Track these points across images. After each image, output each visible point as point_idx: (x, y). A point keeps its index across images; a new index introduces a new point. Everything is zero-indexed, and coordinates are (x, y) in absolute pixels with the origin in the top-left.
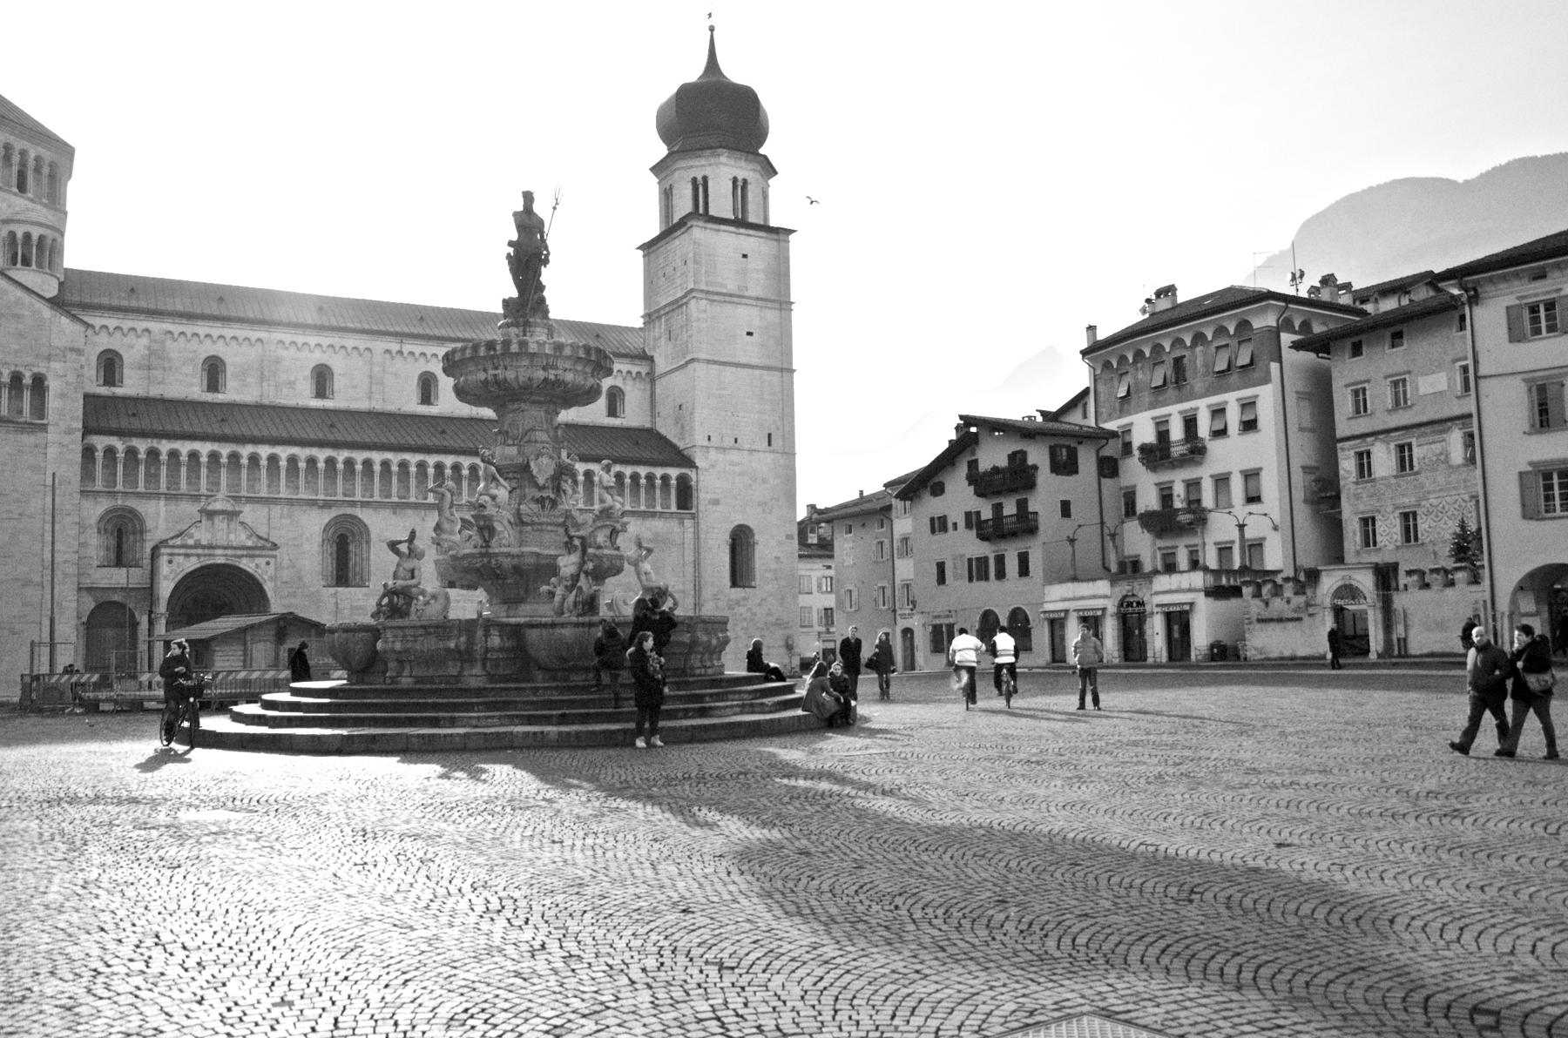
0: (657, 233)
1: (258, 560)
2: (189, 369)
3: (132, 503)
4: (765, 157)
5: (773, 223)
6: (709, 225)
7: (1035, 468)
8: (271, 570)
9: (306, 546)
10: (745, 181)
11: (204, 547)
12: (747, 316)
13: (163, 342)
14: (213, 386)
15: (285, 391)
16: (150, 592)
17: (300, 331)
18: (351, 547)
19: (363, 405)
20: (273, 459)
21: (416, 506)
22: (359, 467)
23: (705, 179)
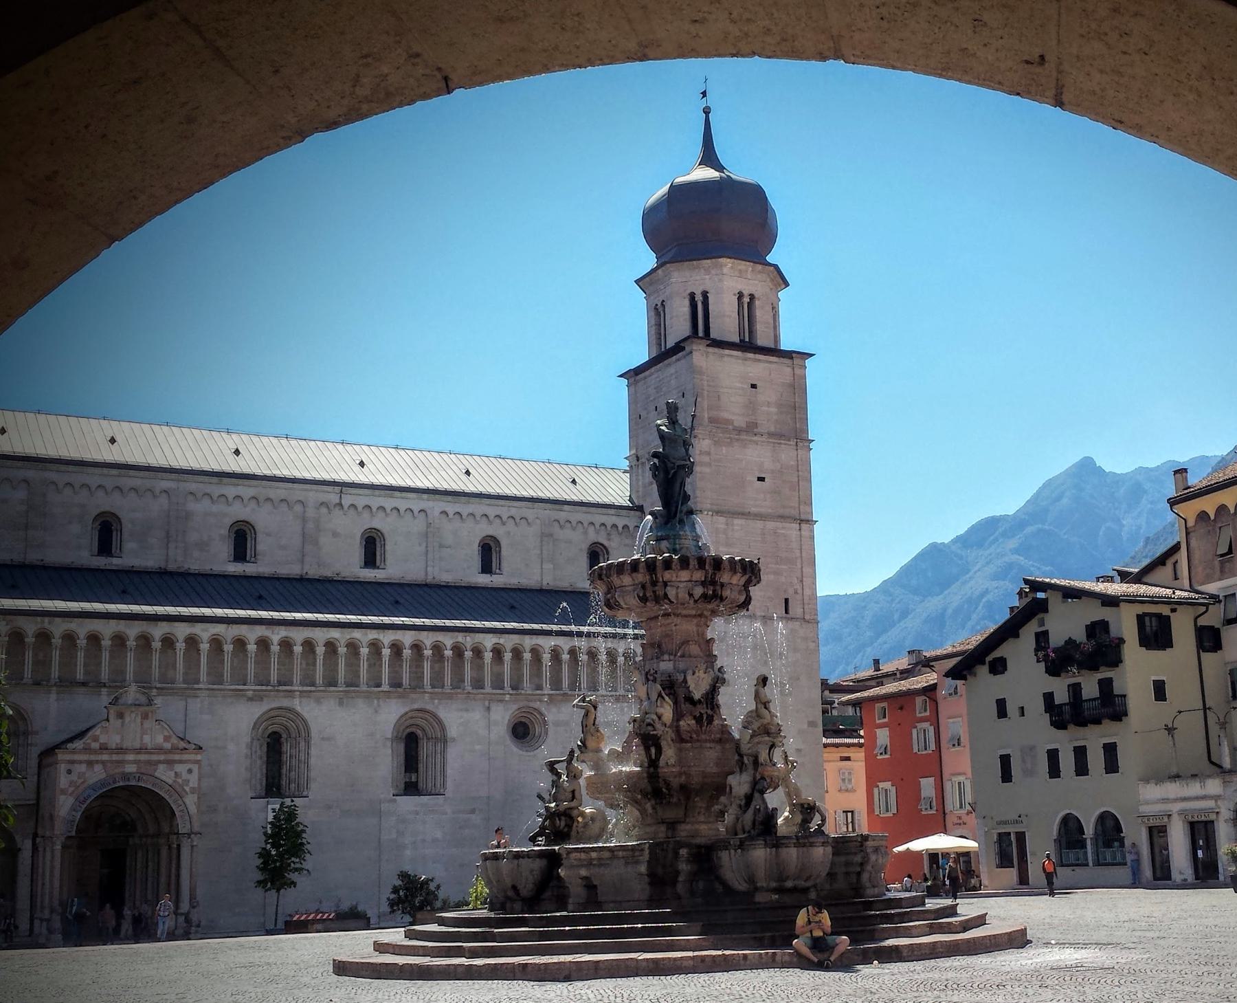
0: (645, 358)
1: (179, 768)
4: (776, 267)
5: (785, 345)
6: (711, 350)
7: (1122, 641)
8: (193, 781)
9: (231, 747)
10: (752, 297)
12: (757, 456)
16: (36, 811)
18: (286, 747)
19: (294, 570)
21: (368, 696)
22: (298, 649)
23: (705, 295)
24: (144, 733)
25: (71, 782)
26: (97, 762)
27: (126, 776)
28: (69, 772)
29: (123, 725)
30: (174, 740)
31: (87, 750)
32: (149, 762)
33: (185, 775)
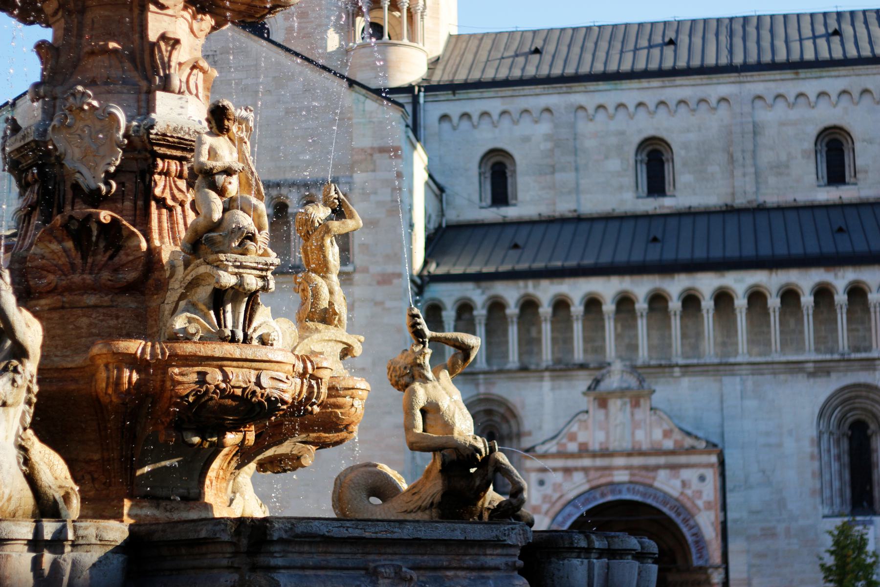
1: (686, 474)
2: (614, 164)
3: (503, 389)
9: (789, 445)
11: (594, 455)
13: (573, 126)
14: (656, 185)
15: (772, 180)
17: (789, 74)
20: (723, 298)
24: (635, 425)
25: (545, 498)
26: (576, 469)
27: (613, 486)
28: (541, 483)
29: (607, 416)
30: (678, 436)
31: (562, 454)
32: (646, 468)
33: (695, 484)
